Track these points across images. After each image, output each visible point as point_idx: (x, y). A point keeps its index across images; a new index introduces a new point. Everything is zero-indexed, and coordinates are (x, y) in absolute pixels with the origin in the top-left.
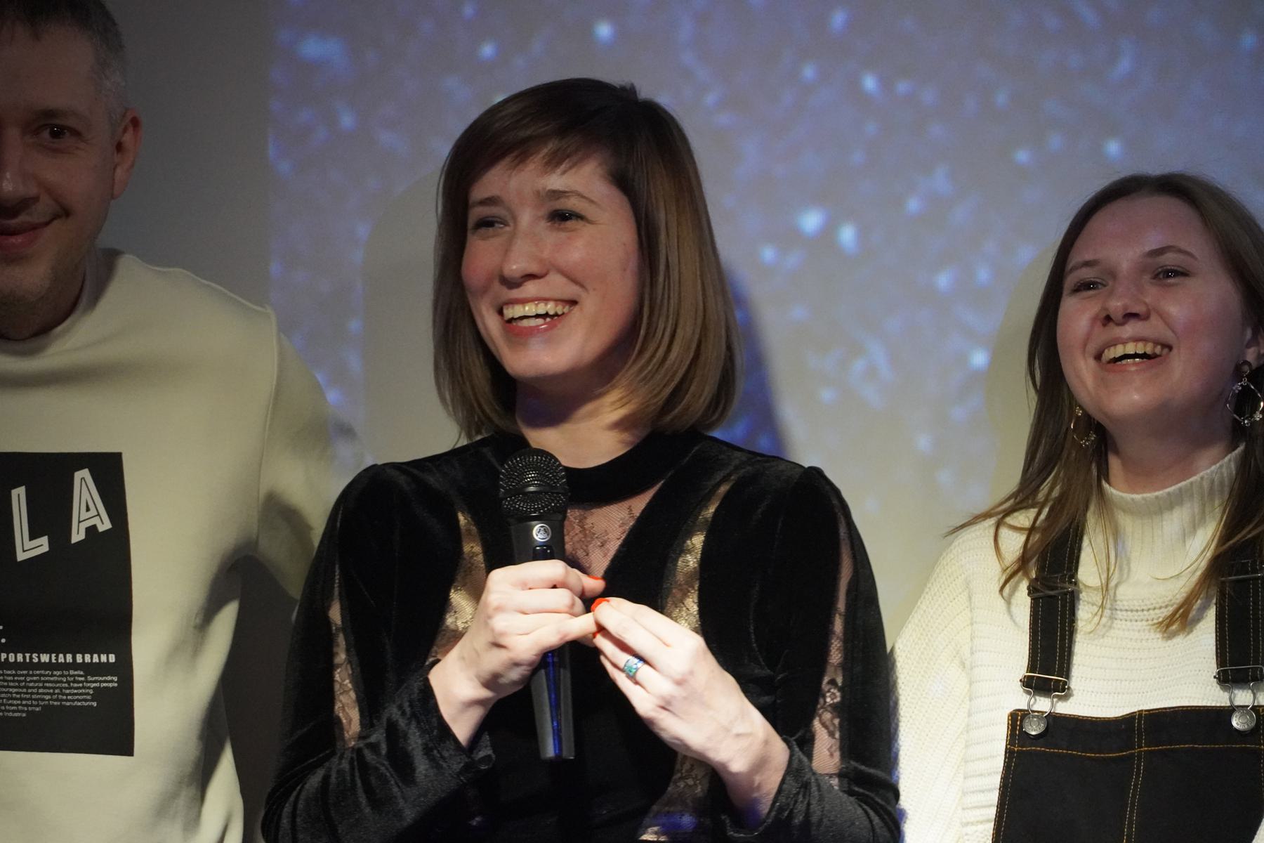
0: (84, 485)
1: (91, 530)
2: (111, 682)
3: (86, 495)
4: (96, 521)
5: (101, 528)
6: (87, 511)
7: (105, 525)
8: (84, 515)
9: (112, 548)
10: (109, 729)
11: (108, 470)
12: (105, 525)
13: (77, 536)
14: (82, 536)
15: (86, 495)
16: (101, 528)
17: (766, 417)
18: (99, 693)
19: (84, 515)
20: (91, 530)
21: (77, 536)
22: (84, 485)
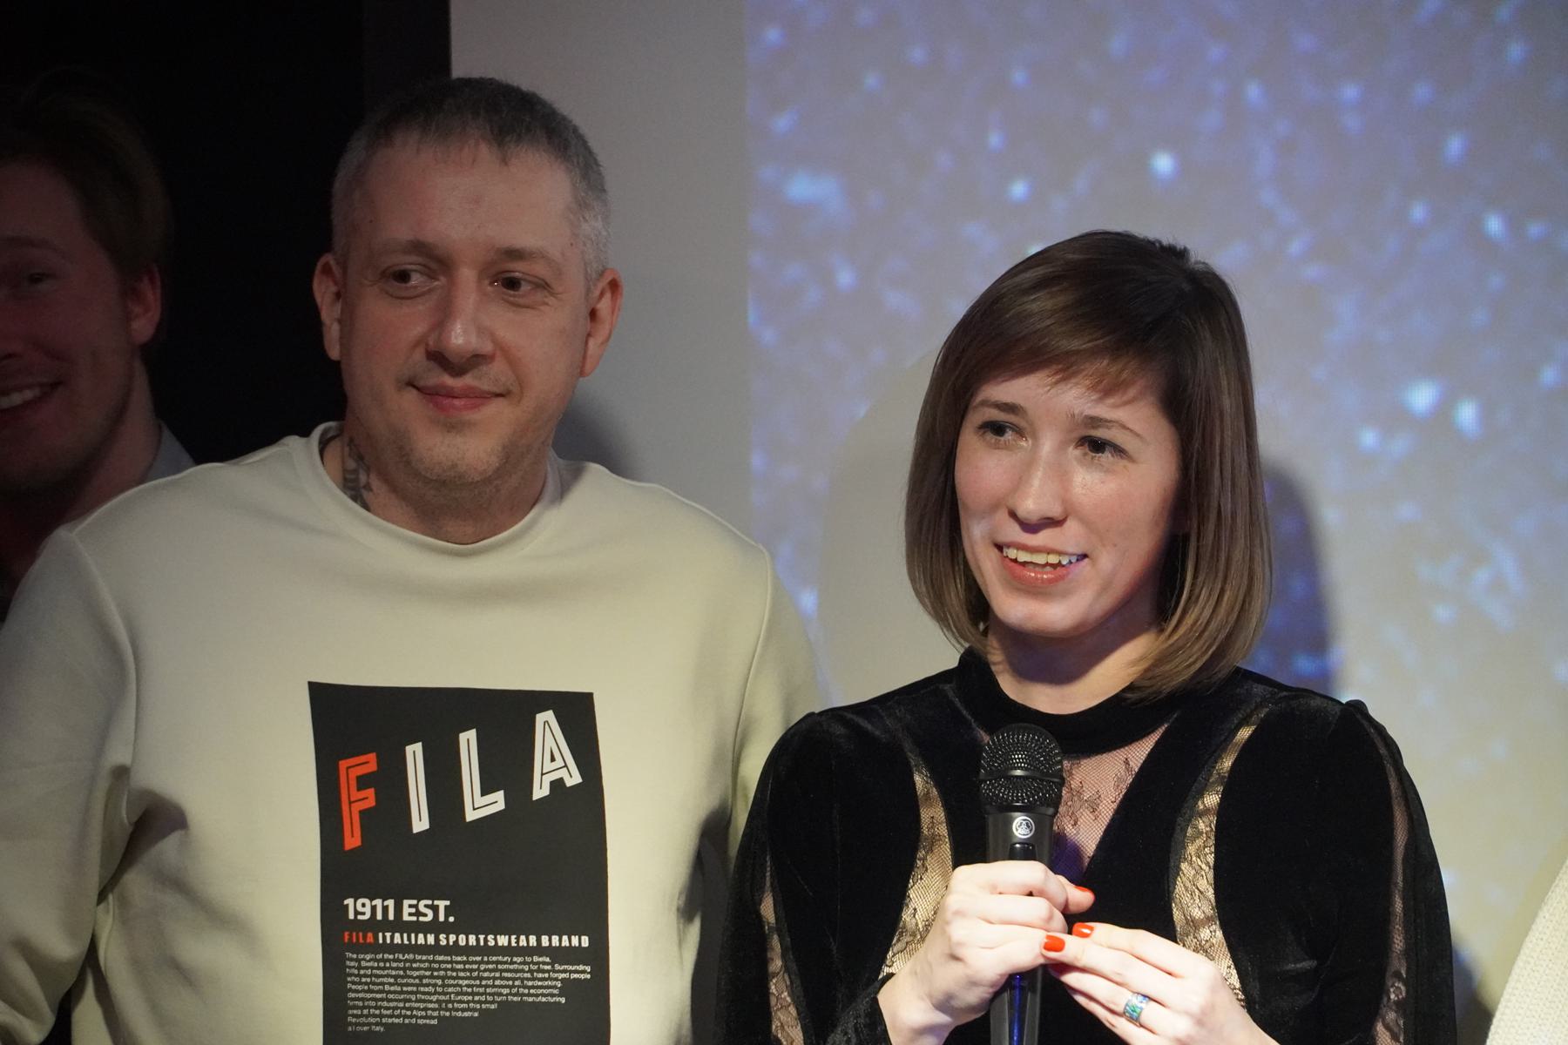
0: (548, 730)
1: (557, 785)
3: (550, 742)
4: (563, 773)
5: (569, 783)
6: (551, 761)
7: (573, 778)
8: (548, 766)
9: (584, 805)
11: (577, 714)
12: (573, 778)
13: (540, 791)
14: (545, 791)
15: (550, 742)
16: (569, 783)
17: (1315, 631)
19: (548, 766)
20: (557, 785)
21: (540, 791)
22: (548, 730)
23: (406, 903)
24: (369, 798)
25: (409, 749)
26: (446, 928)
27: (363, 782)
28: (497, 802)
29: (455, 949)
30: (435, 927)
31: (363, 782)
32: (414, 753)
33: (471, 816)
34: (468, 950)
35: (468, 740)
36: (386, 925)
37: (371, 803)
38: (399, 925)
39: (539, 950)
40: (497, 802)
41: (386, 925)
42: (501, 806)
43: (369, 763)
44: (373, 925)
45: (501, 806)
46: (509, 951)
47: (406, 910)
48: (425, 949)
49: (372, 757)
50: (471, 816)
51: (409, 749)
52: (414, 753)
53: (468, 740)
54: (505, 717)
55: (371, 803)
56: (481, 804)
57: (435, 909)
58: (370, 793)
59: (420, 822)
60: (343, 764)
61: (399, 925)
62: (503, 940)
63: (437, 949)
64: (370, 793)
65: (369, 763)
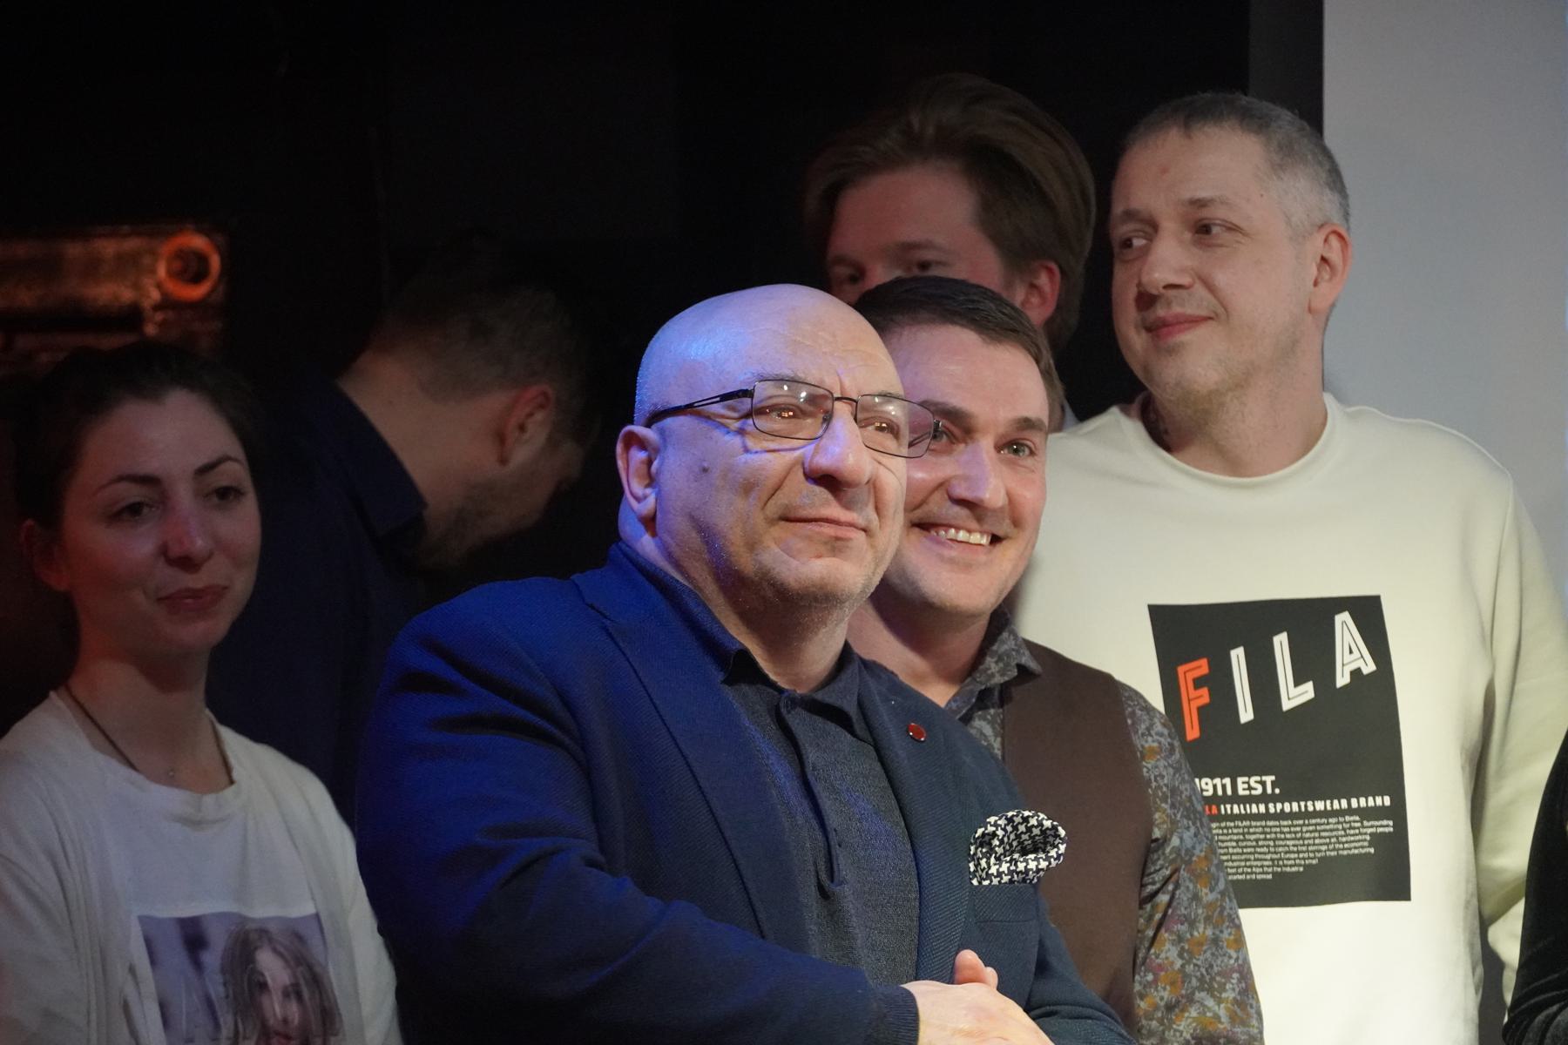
0: (1345, 628)
1: (1356, 673)
4: (1360, 664)
5: (1366, 671)
6: (1350, 655)
7: (1369, 667)
8: (1348, 657)
9: (1378, 689)
11: (1368, 612)
12: (1369, 667)
13: (1342, 679)
16: (1366, 671)
20: (1356, 673)
21: (1342, 679)
22: (1345, 628)
23: (1240, 780)
24: (1204, 697)
26: (1274, 799)
27: (1198, 683)
28: (1307, 692)
29: (1282, 816)
30: (1264, 798)
31: (1198, 683)
32: (1238, 656)
33: (1287, 705)
35: (1281, 642)
36: (1225, 799)
37: (1206, 699)
38: (1236, 799)
40: (1307, 692)
41: (1225, 799)
43: (1201, 667)
44: (1215, 800)
45: (1310, 695)
46: (1325, 814)
48: (1258, 817)
49: (1204, 662)
50: (1287, 705)
52: (1238, 656)
53: (1281, 642)
54: (1309, 621)
55: (1206, 699)
56: (1294, 695)
57: (1263, 784)
58: (1204, 691)
59: (1246, 714)
60: (1181, 669)
61: (1236, 799)
62: (1320, 805)
63: (1267, 816)
64: (1204, 691)
65: (1201, 667)
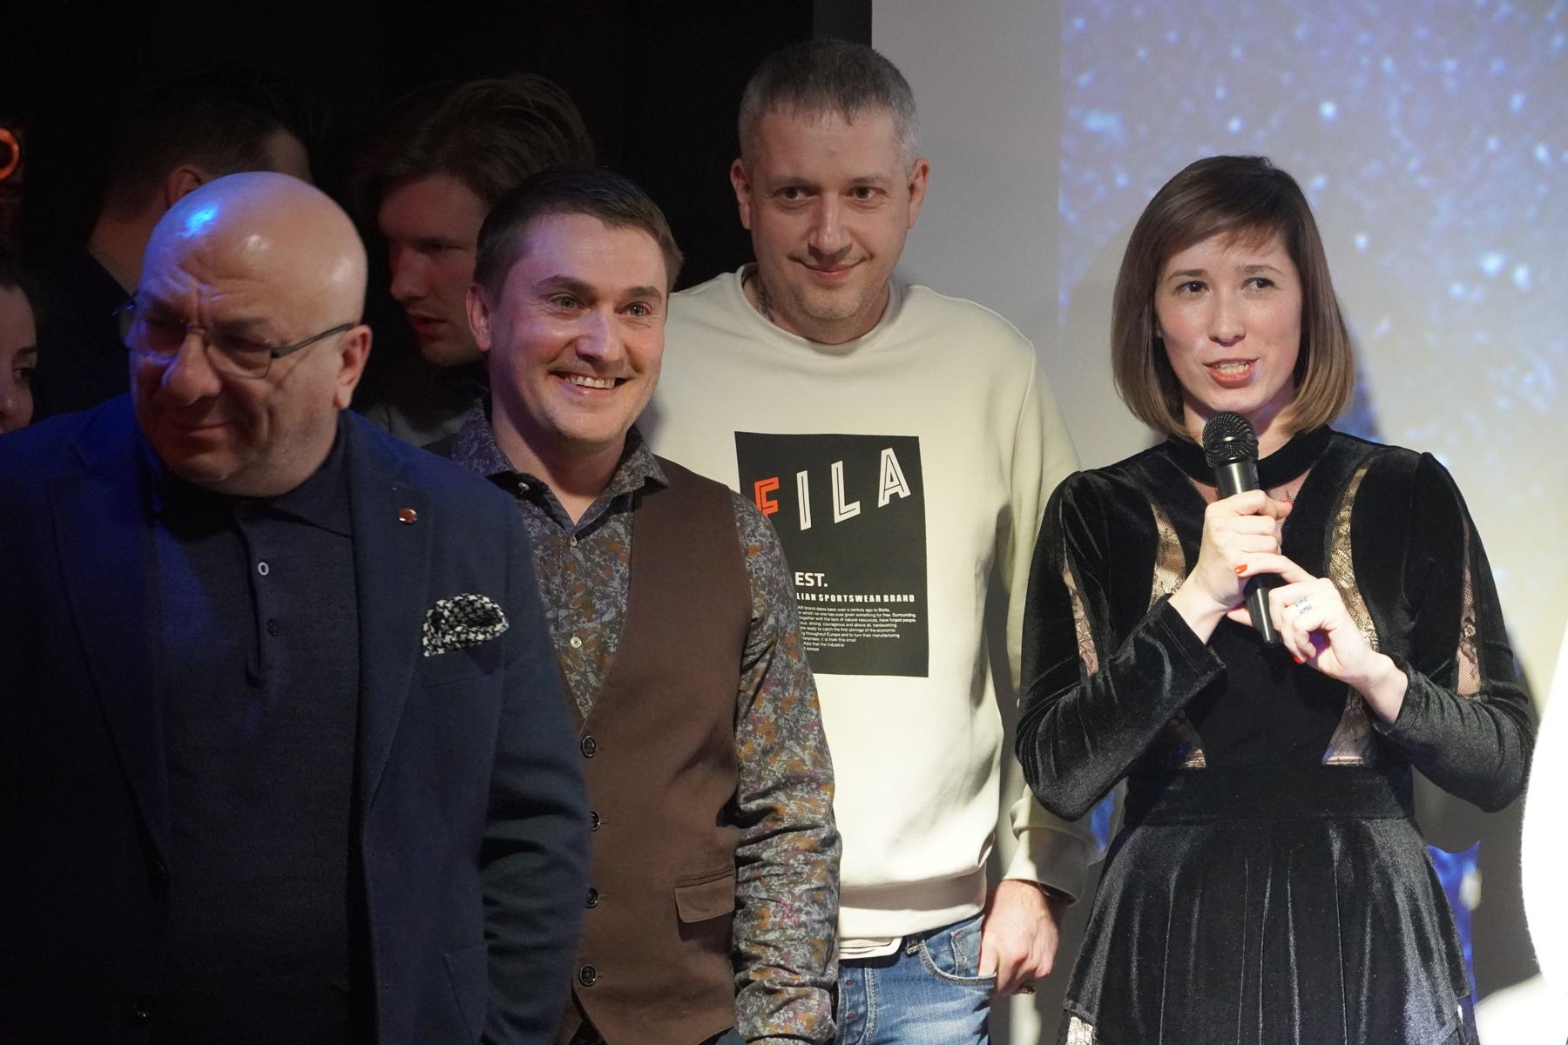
1: (895, 497)
2: (911, 618)
4: (898, 489)
5: (902, 495)
6: (891, 481)
7: (905, 492)
8: (889, 484)
9: (911, 510)
10: (907, 655)
11: (908, 450)
12: (905, 492)
13: (883, 501)
14: (887, 501)
16: (902, 495)
18: (901, 627)
19: (889, 484)
20: (895, 497)
21: (883, 501)
24: (773, 507)
25: (799, 475)
27: (770, 496)
28: (855, 509)
29: (828, 604)
30: (815, 590)
31: (770, 496)
32: (802, 477)
33: (838, 519)
34: (837, 605)
35: (837, 468)
37: (775, 509)
39: (882, 604)
40: (855, 509)
42: (858, 512)
43: (774, 484)
45: (858, 512)
46: (863, 605)
47: (798, 579)
48: (810, 603)
49: (776, 480)
50: (838, 519)
51: (799, 475)
52: (802, 477)
53: (837, 468)
54: (861, 454)
55: (775, 509)
56: (845, 511)
57: (815, 579)
58: (775, 502)
59: (806, 524)
60: (757, 484)
62: (859, 598)
63: (817, 603)
64: (775, 502)
65: (774, 484)
